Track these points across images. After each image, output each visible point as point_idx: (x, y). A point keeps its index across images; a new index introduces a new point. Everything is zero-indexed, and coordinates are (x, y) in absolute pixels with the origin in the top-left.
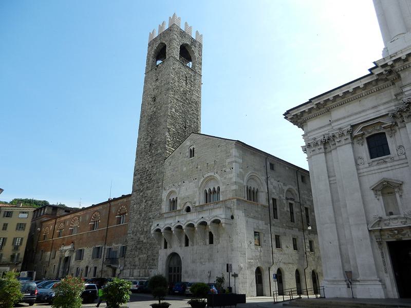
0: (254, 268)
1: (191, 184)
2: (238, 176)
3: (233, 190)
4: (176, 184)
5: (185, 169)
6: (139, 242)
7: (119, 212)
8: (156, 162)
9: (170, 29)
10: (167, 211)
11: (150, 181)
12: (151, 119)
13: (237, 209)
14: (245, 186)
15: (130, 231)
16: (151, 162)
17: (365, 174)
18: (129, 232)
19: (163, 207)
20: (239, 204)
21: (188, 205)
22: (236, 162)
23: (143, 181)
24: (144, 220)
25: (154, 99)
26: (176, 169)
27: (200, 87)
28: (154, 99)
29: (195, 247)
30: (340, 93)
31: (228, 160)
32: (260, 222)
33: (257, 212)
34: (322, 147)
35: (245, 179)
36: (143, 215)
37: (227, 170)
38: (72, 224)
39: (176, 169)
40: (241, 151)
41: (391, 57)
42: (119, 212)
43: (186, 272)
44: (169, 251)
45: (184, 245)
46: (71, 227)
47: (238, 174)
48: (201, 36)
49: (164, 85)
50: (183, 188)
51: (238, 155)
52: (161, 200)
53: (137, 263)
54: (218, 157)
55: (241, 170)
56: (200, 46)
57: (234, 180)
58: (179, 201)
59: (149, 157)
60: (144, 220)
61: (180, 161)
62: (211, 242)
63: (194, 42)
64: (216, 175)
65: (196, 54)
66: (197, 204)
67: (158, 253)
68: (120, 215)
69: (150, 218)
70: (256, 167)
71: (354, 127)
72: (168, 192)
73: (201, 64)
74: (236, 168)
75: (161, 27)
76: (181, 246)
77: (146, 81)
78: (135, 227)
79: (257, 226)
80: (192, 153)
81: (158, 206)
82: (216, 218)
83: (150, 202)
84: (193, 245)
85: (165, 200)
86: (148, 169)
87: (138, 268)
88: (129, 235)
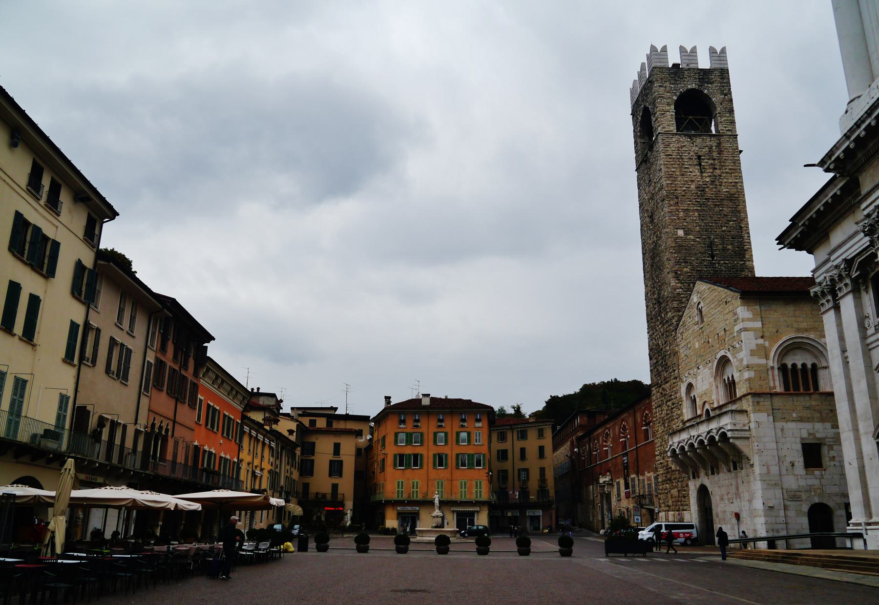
0: (804, 505)
2: (753, 353)
3: (746, 380)
5: (697, 345)
9: (650, 82)
10: (690, 417)
11: (666, 367)
12: (653, 258)
13: (755, 411)
14: (773, 368)
17: (874, 345)
19: (684, 411)
20: (758, 402)
21: (707, 406)
22: (746, 330)
23: (660, 369)
25: (651, 217)
27: (737, 163)
28: (651, 217)
29: (721, 475)
30: (819, 206)
31: (737, 328)
32: (818, 426)
33: (808, 408)
34: (830, 297)
35: (772, 354)
37: (737, 346)
38: (606, 442)
40: (758, 307)
41: (830, 157)
43: (717, 516)
44: (698, 483)
46: (606, 446)
47: (751, 351)
48: (723, 50)
49: (659, 191)
50: (699, 378)
51: (751, 316)
52: (681, 400)
53: (670, 503)
54: (727, 322)
55: (761, 341)
56: (724, 73)
57: (745, 363)
58: (698, 400)
61: (691, 330)
62: (735, 468)
63: (705, 75)
64: (729, 355)
65: (716, 99)
66: (715, 405)
67: (687, 486)
68: (646, 425)
70: (804, 325)
71: (849, 262)
72: (686, 384)
73: (731, 111)
74: (749, 341)
75: (640, 75)
76: (707, 475)
77: (639, 185)
79: (810, 434)
80: (700, 311)
82: (722, 430)
83: (670, 403)
84: (718, 473)
85: (684, 398)
87: (673, 510)
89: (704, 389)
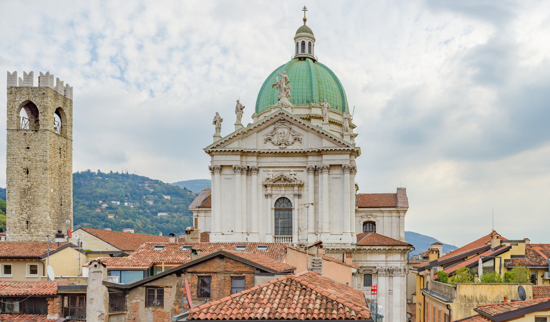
59: (27, 235)
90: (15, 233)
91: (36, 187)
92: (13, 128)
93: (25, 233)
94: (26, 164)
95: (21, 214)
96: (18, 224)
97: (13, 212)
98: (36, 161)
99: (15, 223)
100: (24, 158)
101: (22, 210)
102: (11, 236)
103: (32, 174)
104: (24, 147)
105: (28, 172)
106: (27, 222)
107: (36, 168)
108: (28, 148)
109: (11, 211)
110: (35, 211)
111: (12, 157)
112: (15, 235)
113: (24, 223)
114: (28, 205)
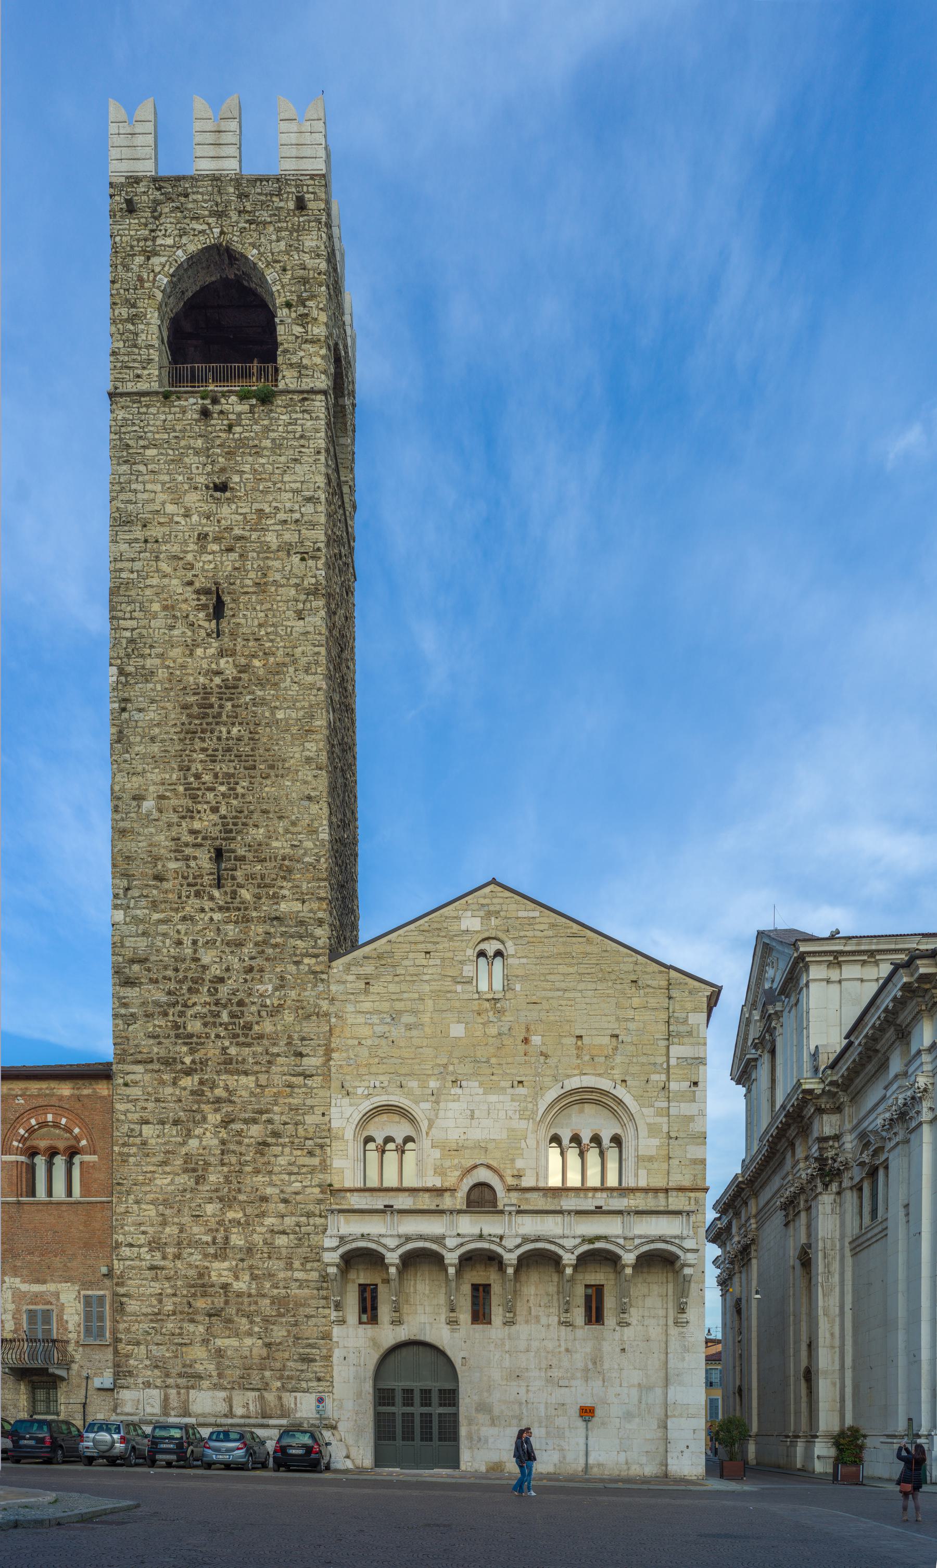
1: (493, 1098)
4: (413, 1084)
6: (202, 1284)
7: (23, 1139)
8: (270, 951)
11: (243, 1033)
15: (127, 1233)
16: (240, 944)
18: (121, 1238)
21: (483, 1175)
23: (195, 1026)
24: (227, 1202)
26: (407, 1019)
36: (212, 1178)
39: (407, 1019)
42: (23, 1139)
45: (465, 1316)
59: (217, 916)
60: (227, 1202)
69: (264, 1199)
72: (366, 1106)
78: (164, 1224)
81: (311, 1154)
83: (255, 1131)
85: (349, 1134)
86: (216, 970)
88: (126, 1251)
89: (476, 1134)
90: (154, 906)
91: (261, 684)
92: (143, 386)
93: (208, 905)
94: (213, 564)
95: (190, 814)
96: (172, 865)
97: (148, 805)
98: (265, 549)
99: (157, 859)
100: (202, 537)
101: (192, 794)
102: (137, 921)
103: (246, 617)
104: (202, 480)
105: (218, 611)
106: (219, 855)
107: (261, 586)
108: (222, 487)
109: (138, 798)
110: (260, 800)
111: (138, 533)
112: (156, 916)
113: (204, 859)
114: (223, 768)
